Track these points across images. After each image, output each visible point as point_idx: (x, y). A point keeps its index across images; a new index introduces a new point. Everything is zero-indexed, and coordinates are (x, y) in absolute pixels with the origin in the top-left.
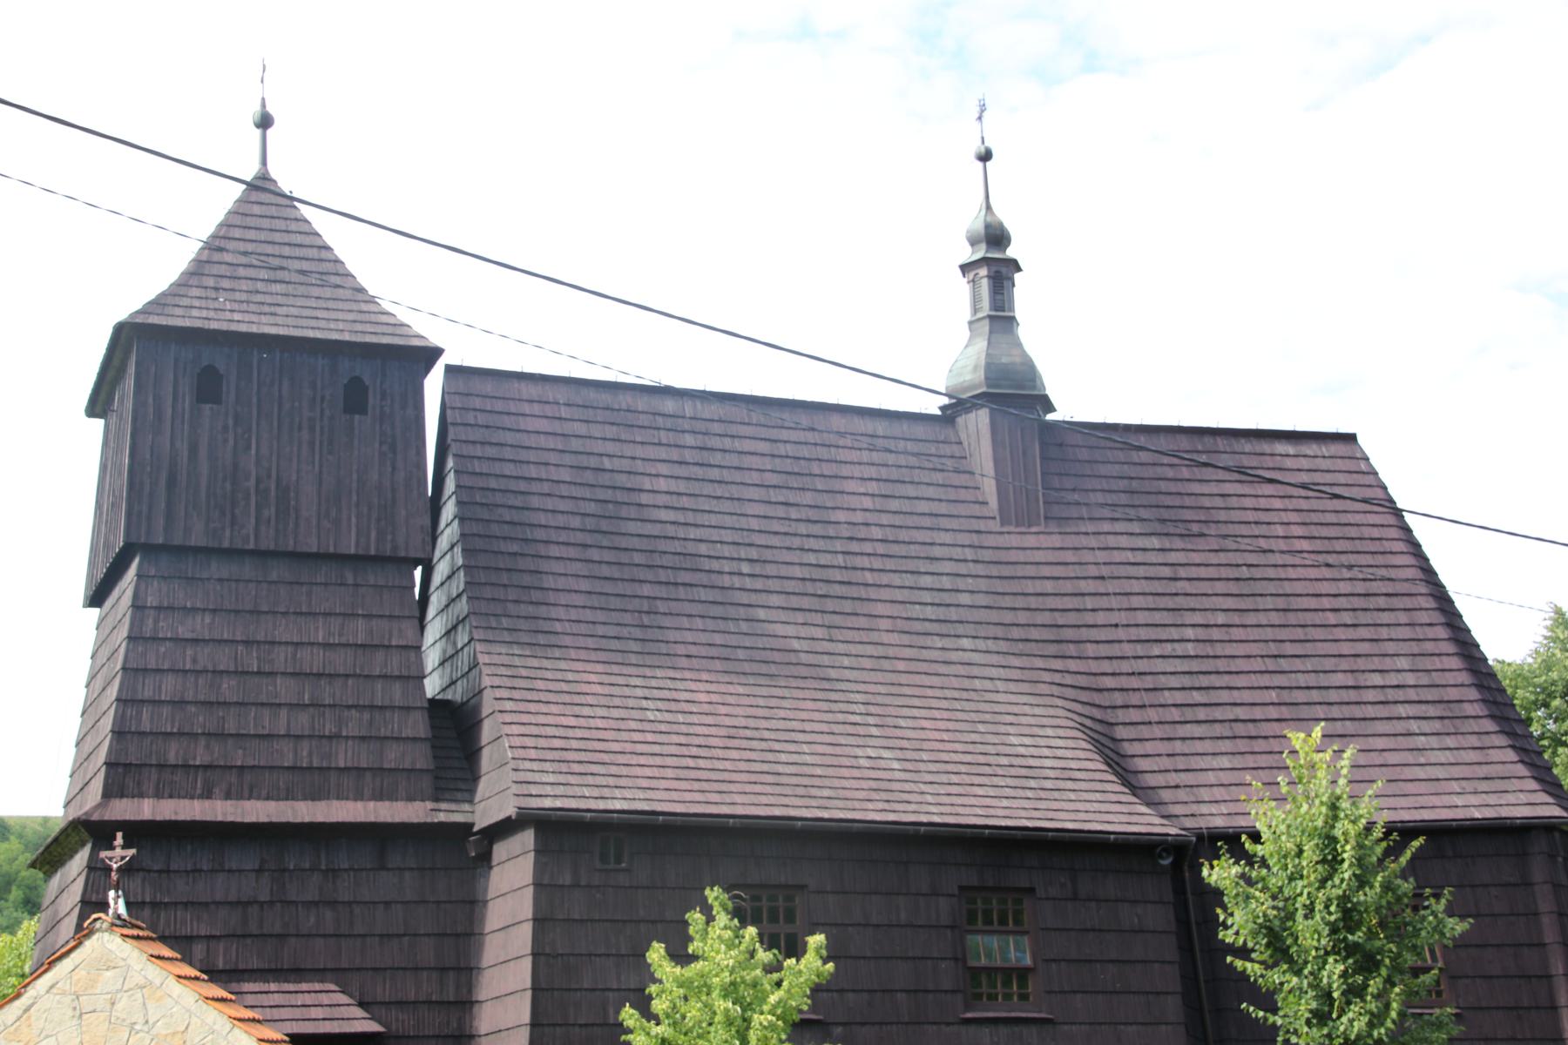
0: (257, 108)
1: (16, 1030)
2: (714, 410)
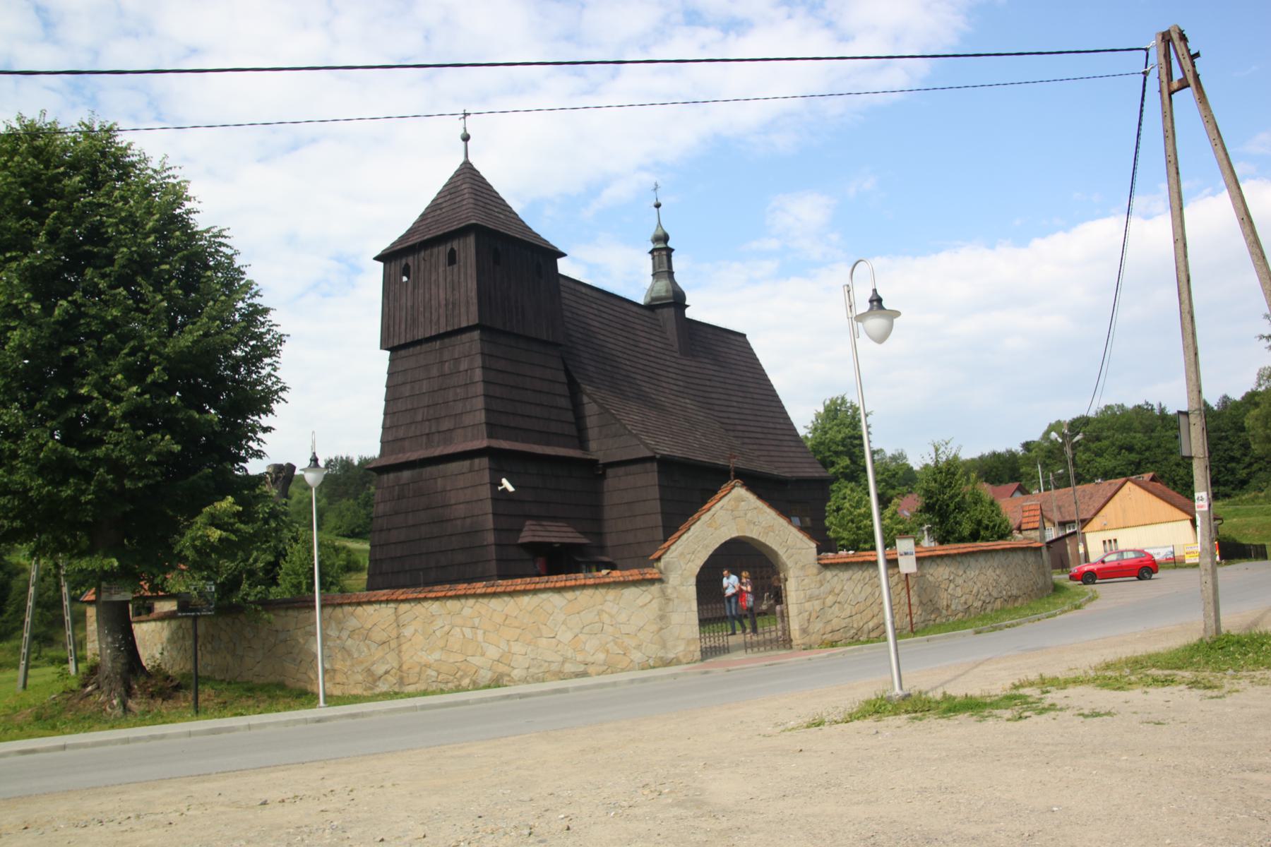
0: (462, 131)
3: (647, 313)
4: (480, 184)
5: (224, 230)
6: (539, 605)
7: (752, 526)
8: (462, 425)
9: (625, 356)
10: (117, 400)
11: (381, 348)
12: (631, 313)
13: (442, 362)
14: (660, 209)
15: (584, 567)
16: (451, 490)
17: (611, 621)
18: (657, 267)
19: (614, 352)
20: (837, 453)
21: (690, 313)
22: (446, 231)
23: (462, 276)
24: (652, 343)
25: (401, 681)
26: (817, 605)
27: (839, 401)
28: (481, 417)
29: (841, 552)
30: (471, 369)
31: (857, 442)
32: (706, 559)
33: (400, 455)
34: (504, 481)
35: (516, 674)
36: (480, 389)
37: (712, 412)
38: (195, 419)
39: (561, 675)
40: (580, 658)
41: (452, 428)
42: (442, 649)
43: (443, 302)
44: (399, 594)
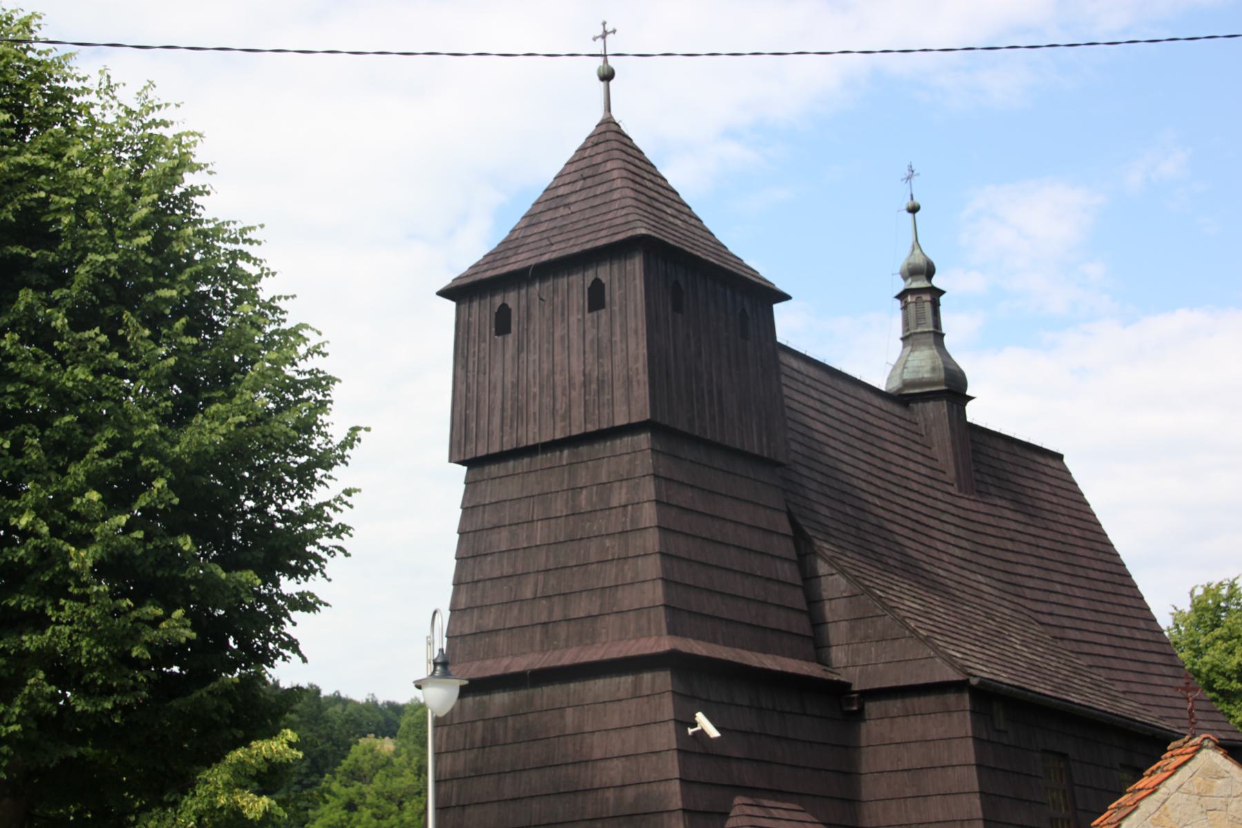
1: (1159, 817)
2: (812, 372)
3: (897, 410)
4: (637, 162)
5: (250, 229)
8: (615, 609)
9: (872, 489)
10: (83, 540)
11: (450, 461)
12: (871, 409)
14: (917, 214)
18: (912, 323)
19: (855, 482)
21: (975, 414)
23: (617, 330)
24: (911, 465)
27: (1224, 592)
28: (655, 593)
33: (489, 663)
34: (700, 717)
36: (652, 540)
37: (1021, 601)
38: (219, 578)
43: (578, 379)
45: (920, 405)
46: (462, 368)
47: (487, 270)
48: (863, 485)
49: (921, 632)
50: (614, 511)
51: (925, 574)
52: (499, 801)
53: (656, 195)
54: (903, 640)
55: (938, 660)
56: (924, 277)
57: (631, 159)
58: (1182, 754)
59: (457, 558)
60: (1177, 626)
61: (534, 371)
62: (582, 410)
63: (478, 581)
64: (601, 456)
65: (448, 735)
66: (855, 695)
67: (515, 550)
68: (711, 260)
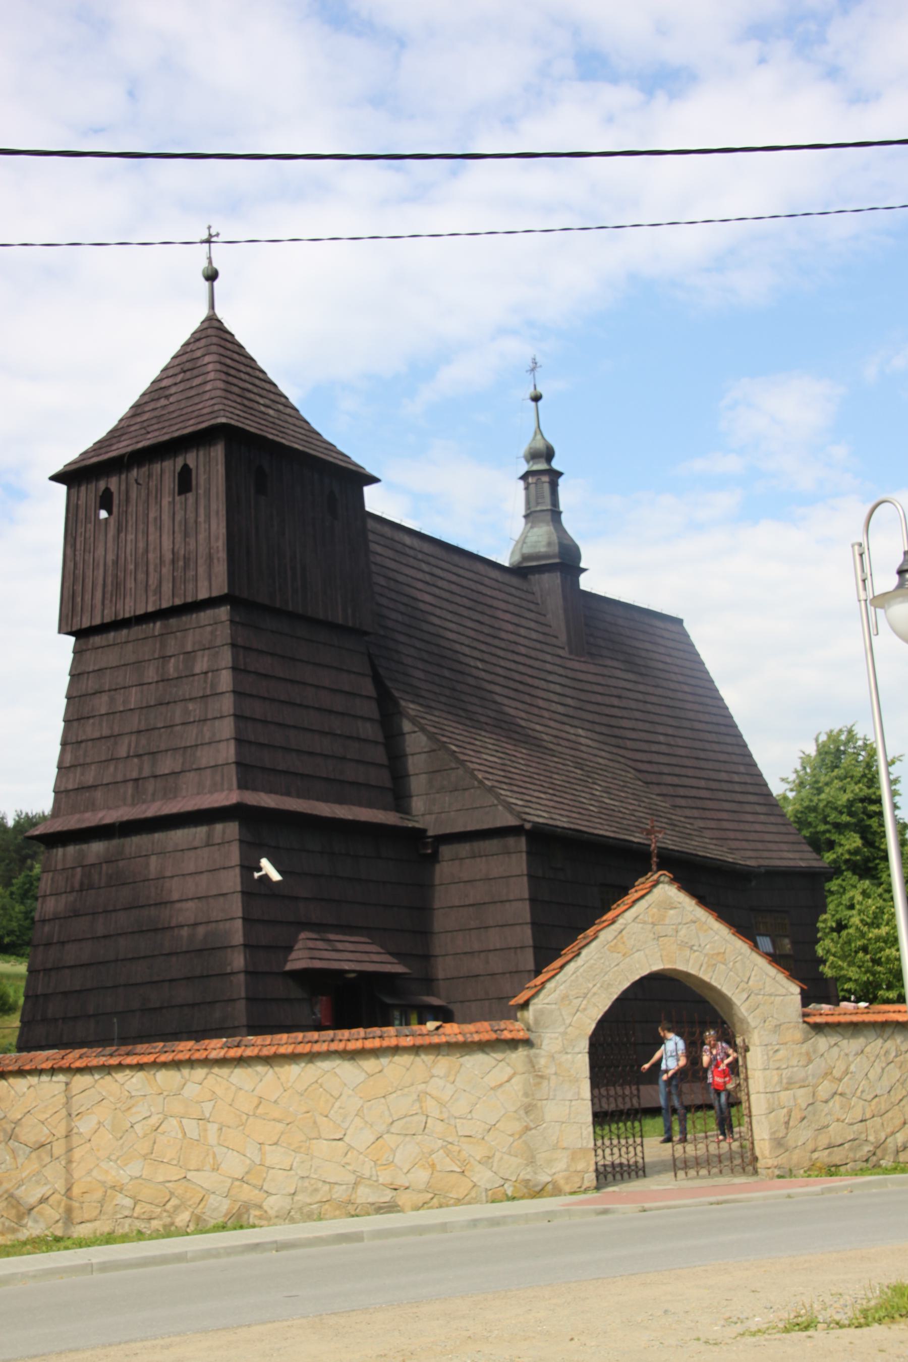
1: (616, 945)
2: (426, 547)
3: (514, 581)
4: (236, 357)
6: (316, 1082)
7: (687, 952)
8: (194, 767)
11: (60, 632)
12: (487, 581)
13: (165, 658)
14: (540, 403)
15: (397, 1014)
16: (172, 877)
17: (441, 1112)
19: (457, 647)
20: (839, 827)
21: (586, 583)
22: (176, 434)
23: (202, 511)
24: (522, 631)
25: (69, 1218)
26: (802, 1096)
28: (228, 752)
29: (844, 1004)
30: (213, 671)
31: (874, 808)
32: (607, 1008)
33: (88, 815)
34: (265, 863)
35: (273, 1204)
36: (227, 704)
37: (621, 752)
39: (351, 1208)
40: (384, 1177)
41: (177, 770)
42: (145, 1157)
43: (168, 556)
44: (73, 1057)
45: (537, 576)
46: (71, 547)
47: (92, 457)
48: (467, 651)
49: (487, 782)
50: (196, 678)
51: (519, 730)
52: (93, 938)
53: (250, 387)
54: (472, 790)
55: (500, 808)
56: (543, 460)
57: (229, 353)
58: (642, 889)
59: (65, 721)
60: (804, 768)
61: (131, 550)
62: (171, 585)
63: (81, 742)
64: (187, 627)
65: (52, 879)
66: (430, 840)
67: (113, 713)
68: (296, 446)
